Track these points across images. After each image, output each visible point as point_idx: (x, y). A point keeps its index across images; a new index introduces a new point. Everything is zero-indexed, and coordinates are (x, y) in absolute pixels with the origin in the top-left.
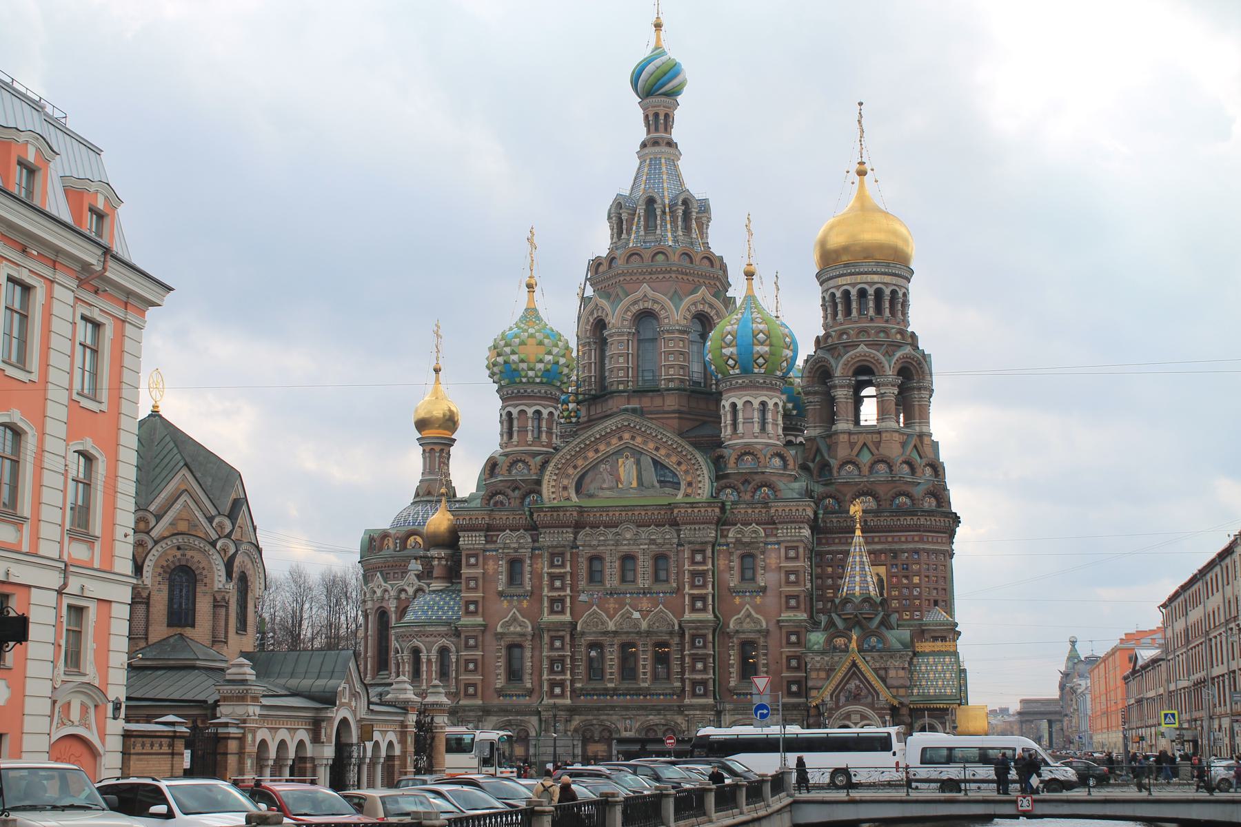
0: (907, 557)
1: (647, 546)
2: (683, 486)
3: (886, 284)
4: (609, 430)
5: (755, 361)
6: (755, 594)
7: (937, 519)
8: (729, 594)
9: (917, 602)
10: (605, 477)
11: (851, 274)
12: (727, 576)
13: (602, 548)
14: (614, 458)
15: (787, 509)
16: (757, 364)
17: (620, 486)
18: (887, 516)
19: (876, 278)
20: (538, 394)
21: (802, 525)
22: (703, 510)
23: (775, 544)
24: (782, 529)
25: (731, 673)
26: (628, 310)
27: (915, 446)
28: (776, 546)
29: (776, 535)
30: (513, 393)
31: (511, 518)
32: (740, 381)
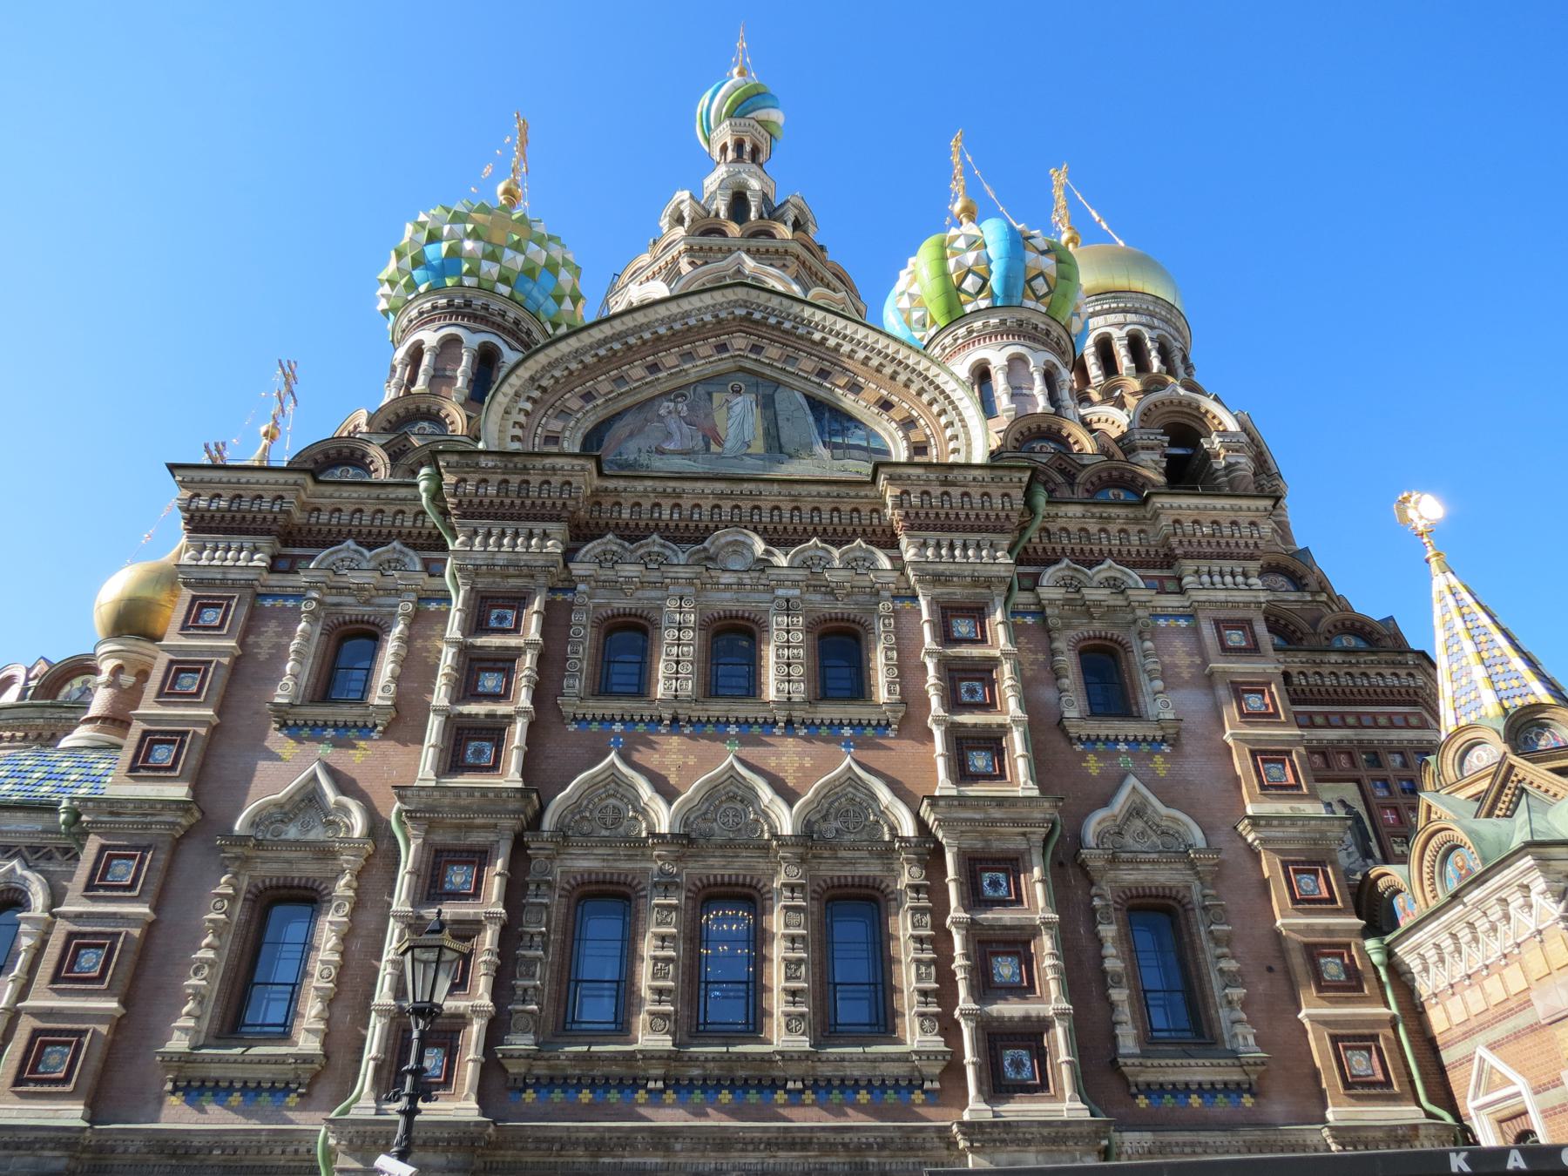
1: (797, 592)
4: (692, 322)
5: (1029, 282)
6: (1145, 748)
8: (1063, 744)
10: (673, 427)
12: (1048, 694)
13: (653, 594)
14: (701, 389)
17: (714, 448)
19: (1156, 322)
20: (499, 319)
21: (1253, 566)
24: (1197, 572)
25: (1112, 1006)
28: (1183, 623)
29: (1182, 591)
30: (434, 308)
31: (369, 510)
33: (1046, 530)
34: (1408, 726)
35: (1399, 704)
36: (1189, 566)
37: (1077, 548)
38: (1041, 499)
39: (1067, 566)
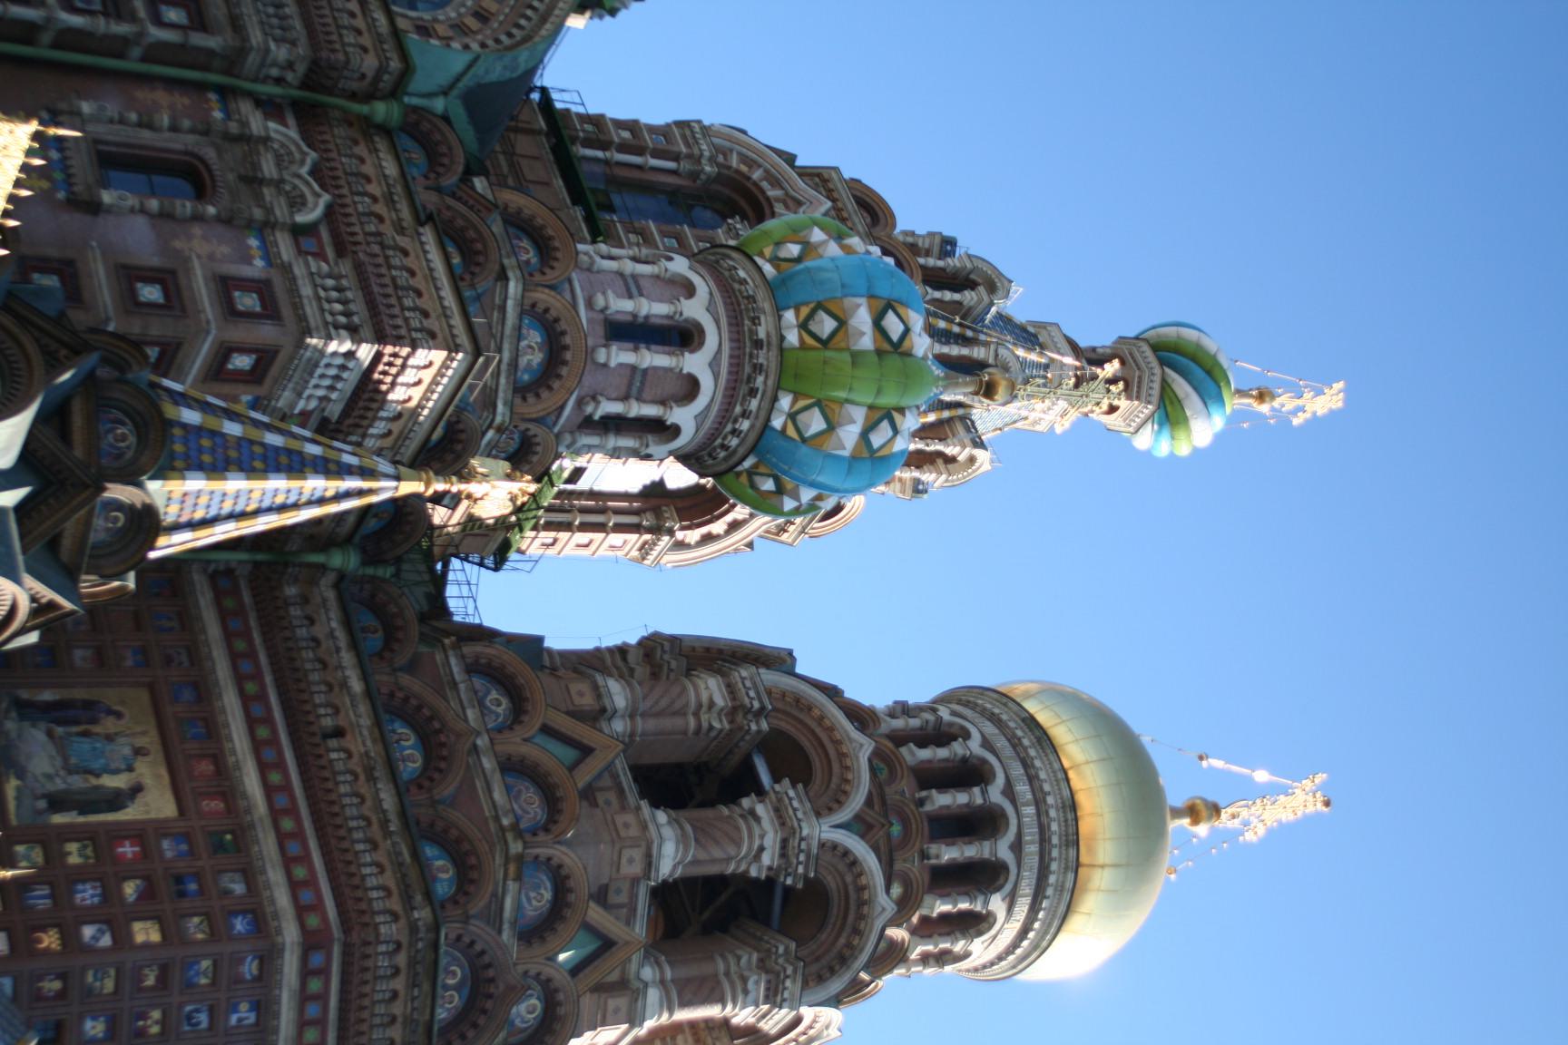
0: (227, 893)
2: (412, 14)
3: (1017, 847)
5: (820, 306)
6: (58, 176)
7: (397, 1009)
9: (50, 940)
11: (1015, 743)
12: (112, 109)
15: (418, 282)
16: (811, 316)
18: (378, 802)
19: (1029, 810)
21: (366, 331)
22: (359, 23)
23: (267, 257)
24: (338, 277)
26: (752, 164)
27: (607, 944)
28: (259, 263)
32: (742, 274)
33: (356, 143)
34: (301, 911)
35: (340, 904)
36: (345, 267)
37: (340, 173)
38: (380, 110)
39: (305, 154)
